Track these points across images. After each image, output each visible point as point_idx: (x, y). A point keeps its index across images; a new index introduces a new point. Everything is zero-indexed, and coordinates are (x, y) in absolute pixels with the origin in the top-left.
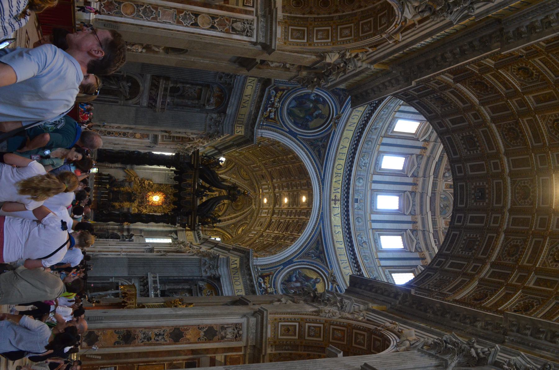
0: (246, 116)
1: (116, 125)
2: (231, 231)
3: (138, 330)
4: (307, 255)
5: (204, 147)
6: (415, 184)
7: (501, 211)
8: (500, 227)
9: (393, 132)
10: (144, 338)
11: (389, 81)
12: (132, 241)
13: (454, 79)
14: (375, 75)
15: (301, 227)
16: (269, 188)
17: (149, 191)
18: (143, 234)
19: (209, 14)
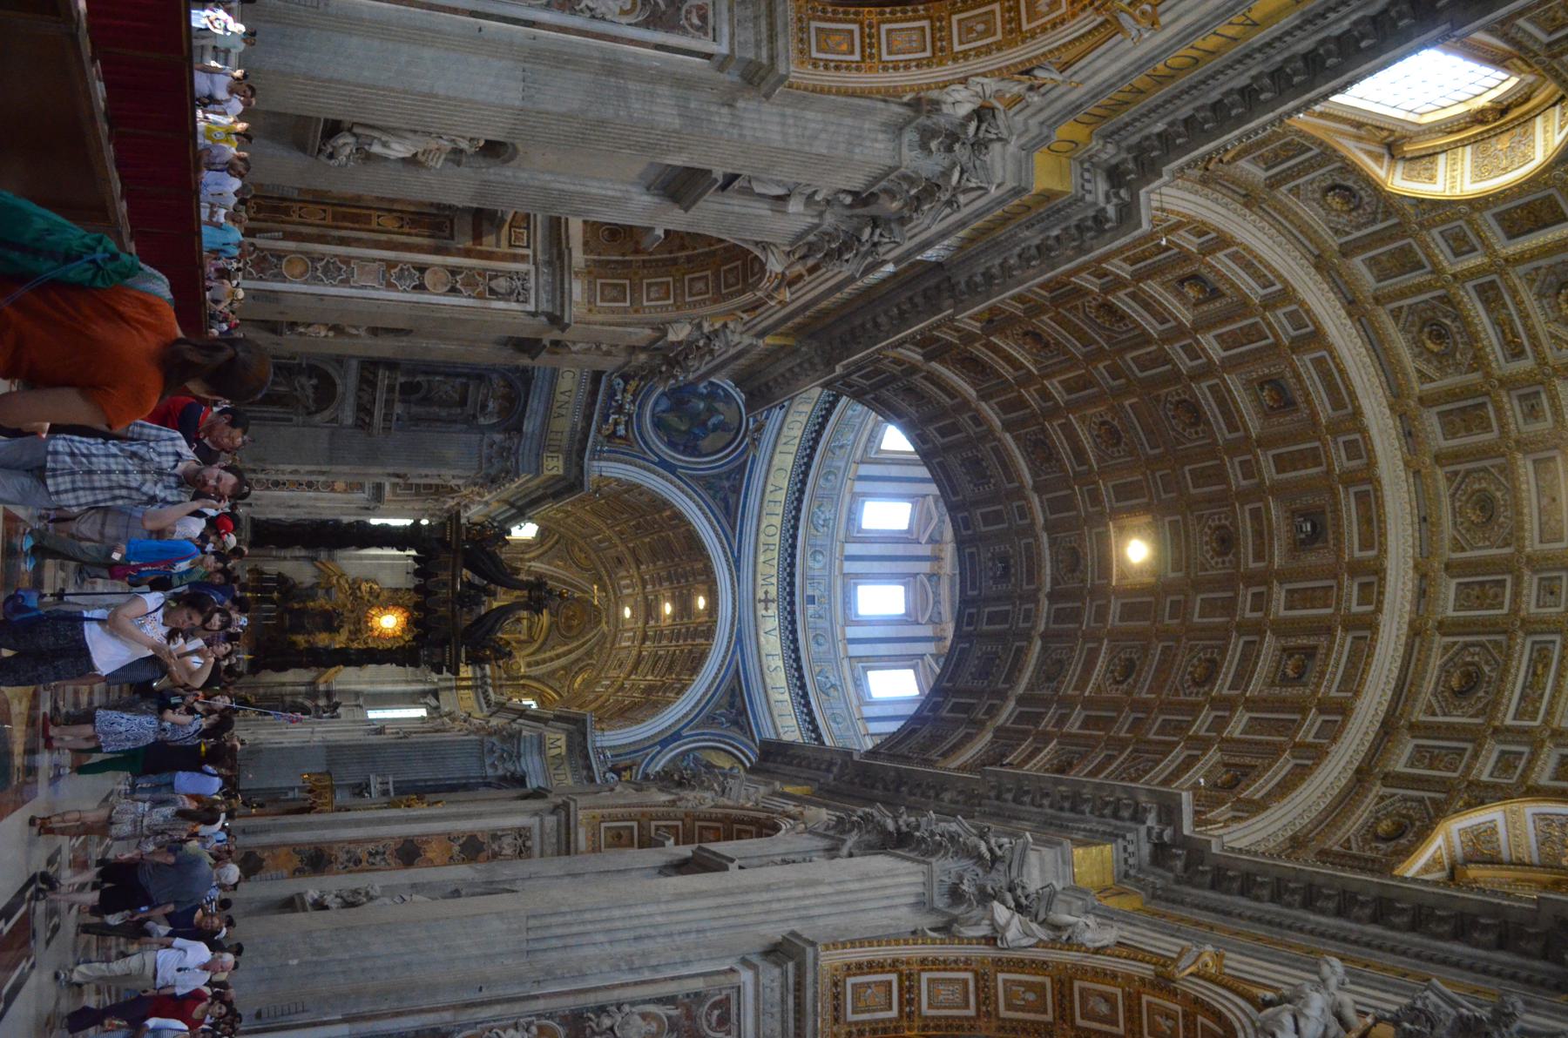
0: (566, 435)
1: (290, 468)
2: (557, 685)
3: (336, 847)
4: (711, 719)
5: (487, 504)
6: (936, 558)
7: (1033, 597)
8: (1033, 628)
9: (879, 451)
10: (349, 861)
11: (800, 365)
12: (338, 716)
13: (923, 355)
14: (773, 354)
15: (695, 662)
16: (632, 586)
17: (372, 606)
18: (361, 701)
19: (445, 267)
